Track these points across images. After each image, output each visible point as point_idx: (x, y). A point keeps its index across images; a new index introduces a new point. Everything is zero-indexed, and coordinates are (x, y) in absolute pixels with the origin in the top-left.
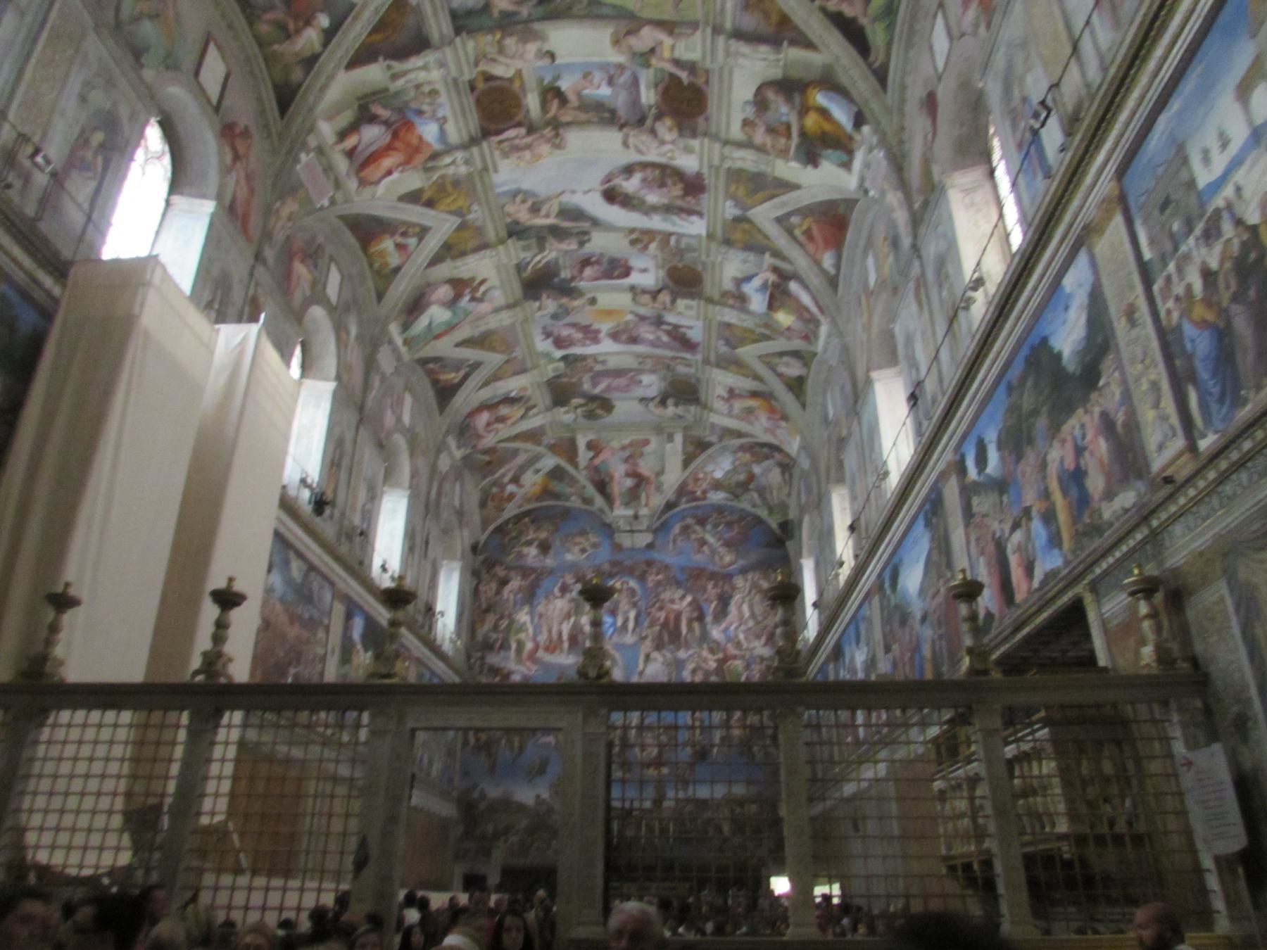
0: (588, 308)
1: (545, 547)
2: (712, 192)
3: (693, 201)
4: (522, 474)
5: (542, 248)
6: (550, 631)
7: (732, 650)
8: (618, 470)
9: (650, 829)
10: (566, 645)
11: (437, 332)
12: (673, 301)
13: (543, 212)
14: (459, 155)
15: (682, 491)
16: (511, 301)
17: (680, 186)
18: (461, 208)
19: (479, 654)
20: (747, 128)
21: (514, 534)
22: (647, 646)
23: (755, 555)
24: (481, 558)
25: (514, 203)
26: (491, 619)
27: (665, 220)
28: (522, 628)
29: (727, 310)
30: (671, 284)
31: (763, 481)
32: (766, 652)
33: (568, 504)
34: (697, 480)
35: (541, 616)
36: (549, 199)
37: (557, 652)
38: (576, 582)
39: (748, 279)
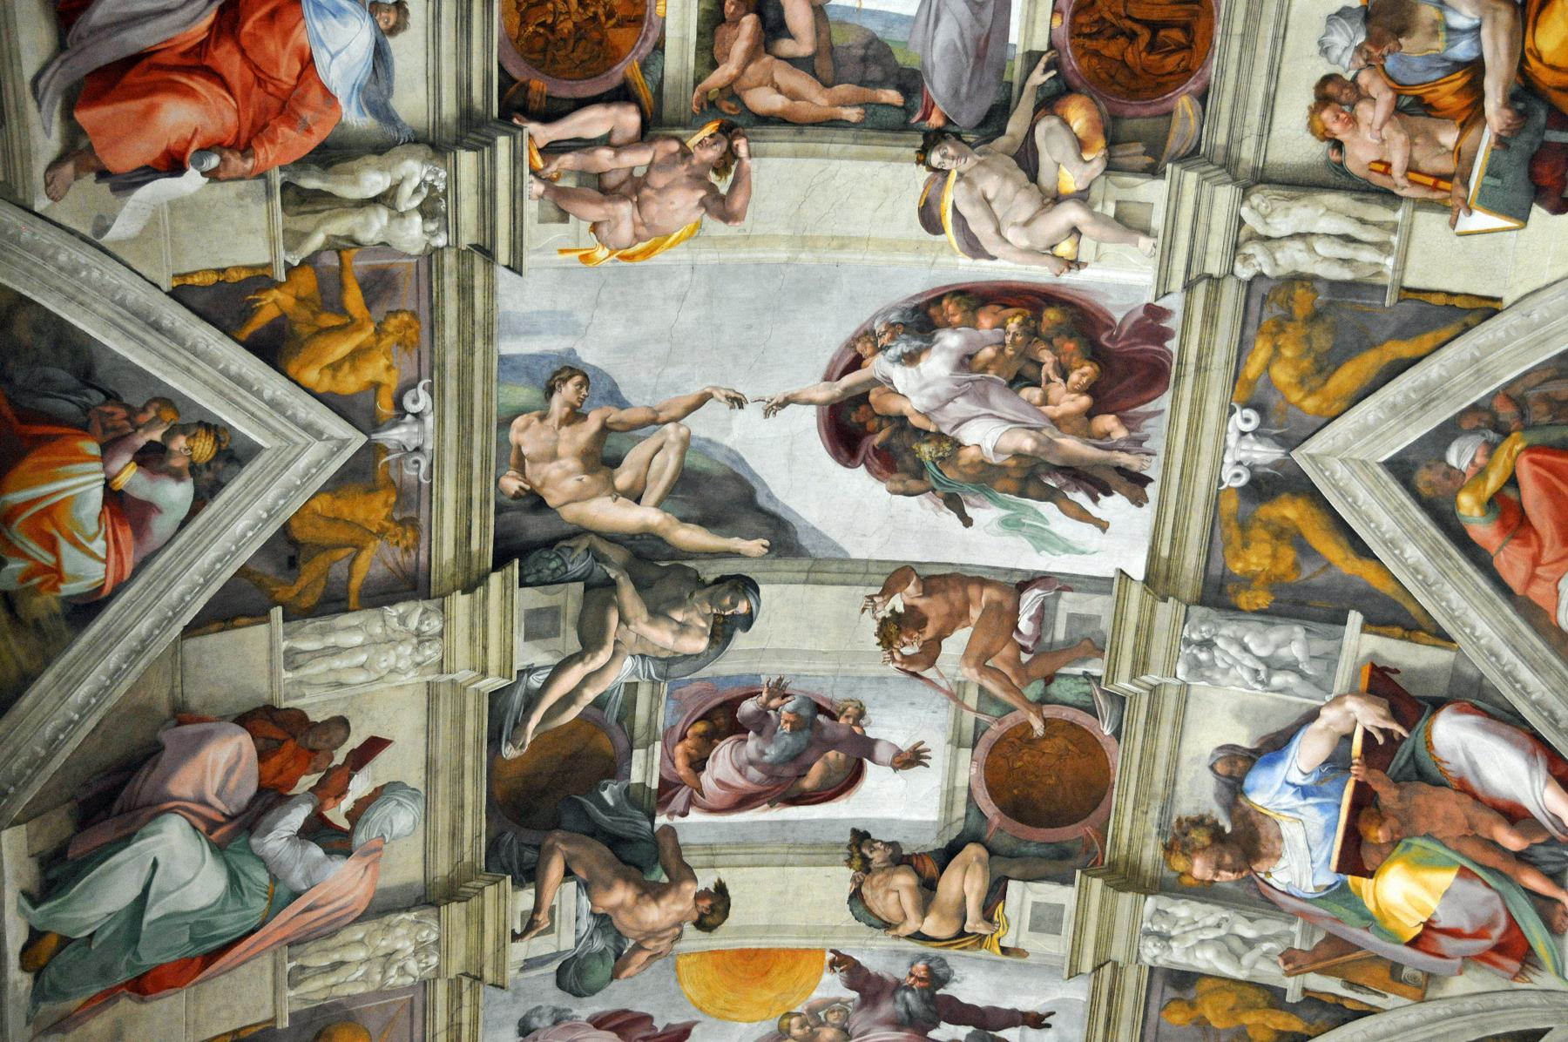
0: (694, 940)
2: (1188, 382)
3: (1120, 433)
5: (591, 640)
11: (150, 956)
12: (995, 894)
13: (623, 479)
14: (414, 170)
16: (442, 868)
17: (1083, 373)
18: (376, 386)
20: (1327, 115)
25: (542, 418)
27: (1011, 525)
29: (1183, 910)
30: (990, 809)
36: (655, 421)
39: (1275, 746)
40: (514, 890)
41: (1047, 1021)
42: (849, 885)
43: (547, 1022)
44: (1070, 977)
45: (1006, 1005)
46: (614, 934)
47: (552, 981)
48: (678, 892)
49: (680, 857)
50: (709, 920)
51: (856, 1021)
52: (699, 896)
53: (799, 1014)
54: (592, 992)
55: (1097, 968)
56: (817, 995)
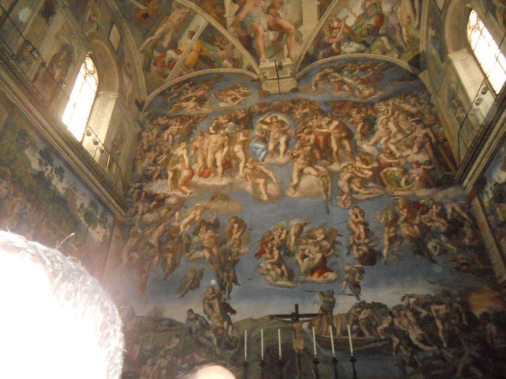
1: (201, 101)
4: (180, 37)
6: (205, 160)
7: (384, 159)
8: (262, 23)
9: (324, 343)
10: (220, 170)
15: (320, 43)
19: (138, 185)
21: (176, 95)
22: (299, 163)
23: (390, 89)
24: (146, 114)
26: (152, 155)
28: (180, 160)
31: (392, 20)
32: (422, 158)
33: (221, 70)
34: (332, 29)
35: (196, 149)
37: (212, 175)
38: (229, 121)
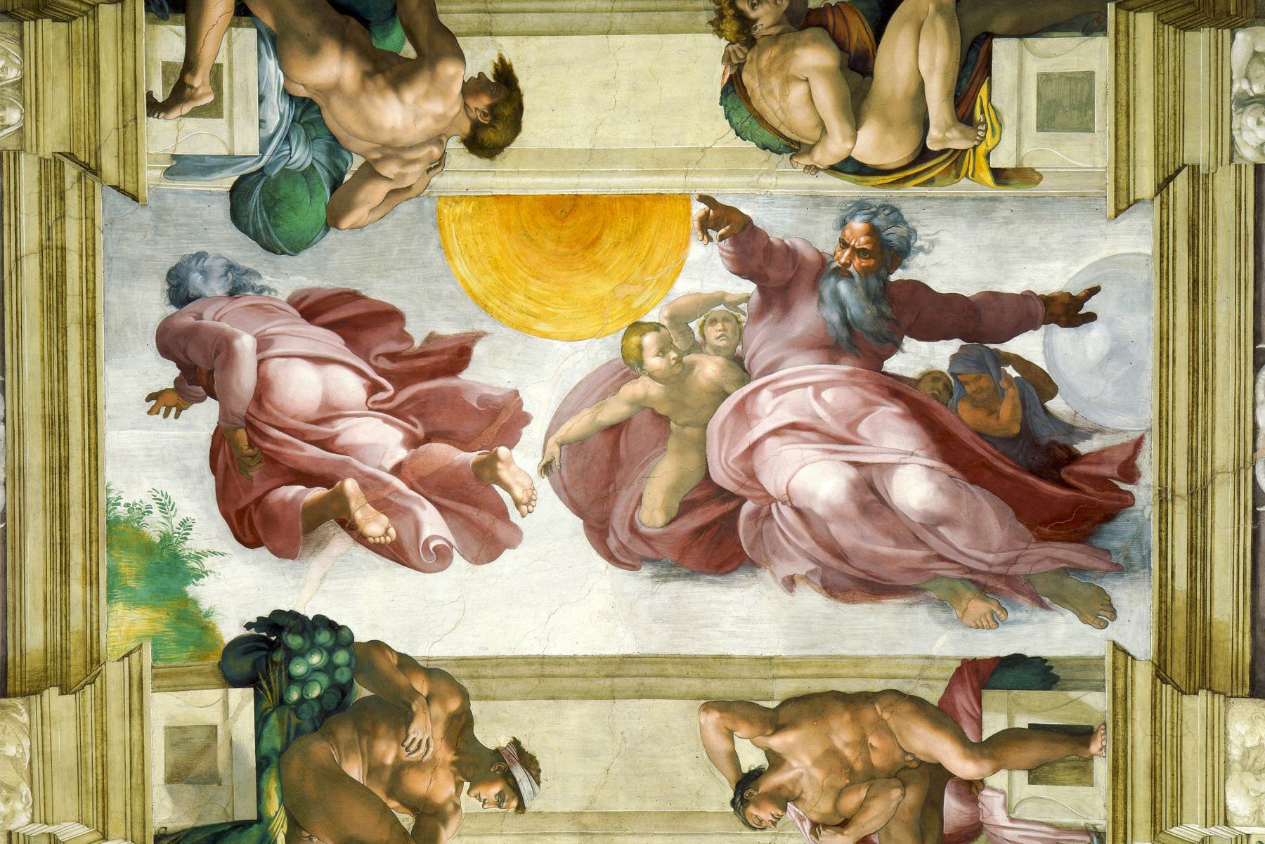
40: (150, 22)
41: (1089, 307)
42: (720, 68)
43: (217, 288)
44: (1118, 212)
45: (1014, 286)
46: (327, 140)
47: (221, 210)
48: (433, 78)
49: (433, 13)
50: (490, 136)
51: (755, 343)
52: (472, 88)
53: (656, 327)
54: (296, 247)
55: (1163, 186)
56: (686, 286)
